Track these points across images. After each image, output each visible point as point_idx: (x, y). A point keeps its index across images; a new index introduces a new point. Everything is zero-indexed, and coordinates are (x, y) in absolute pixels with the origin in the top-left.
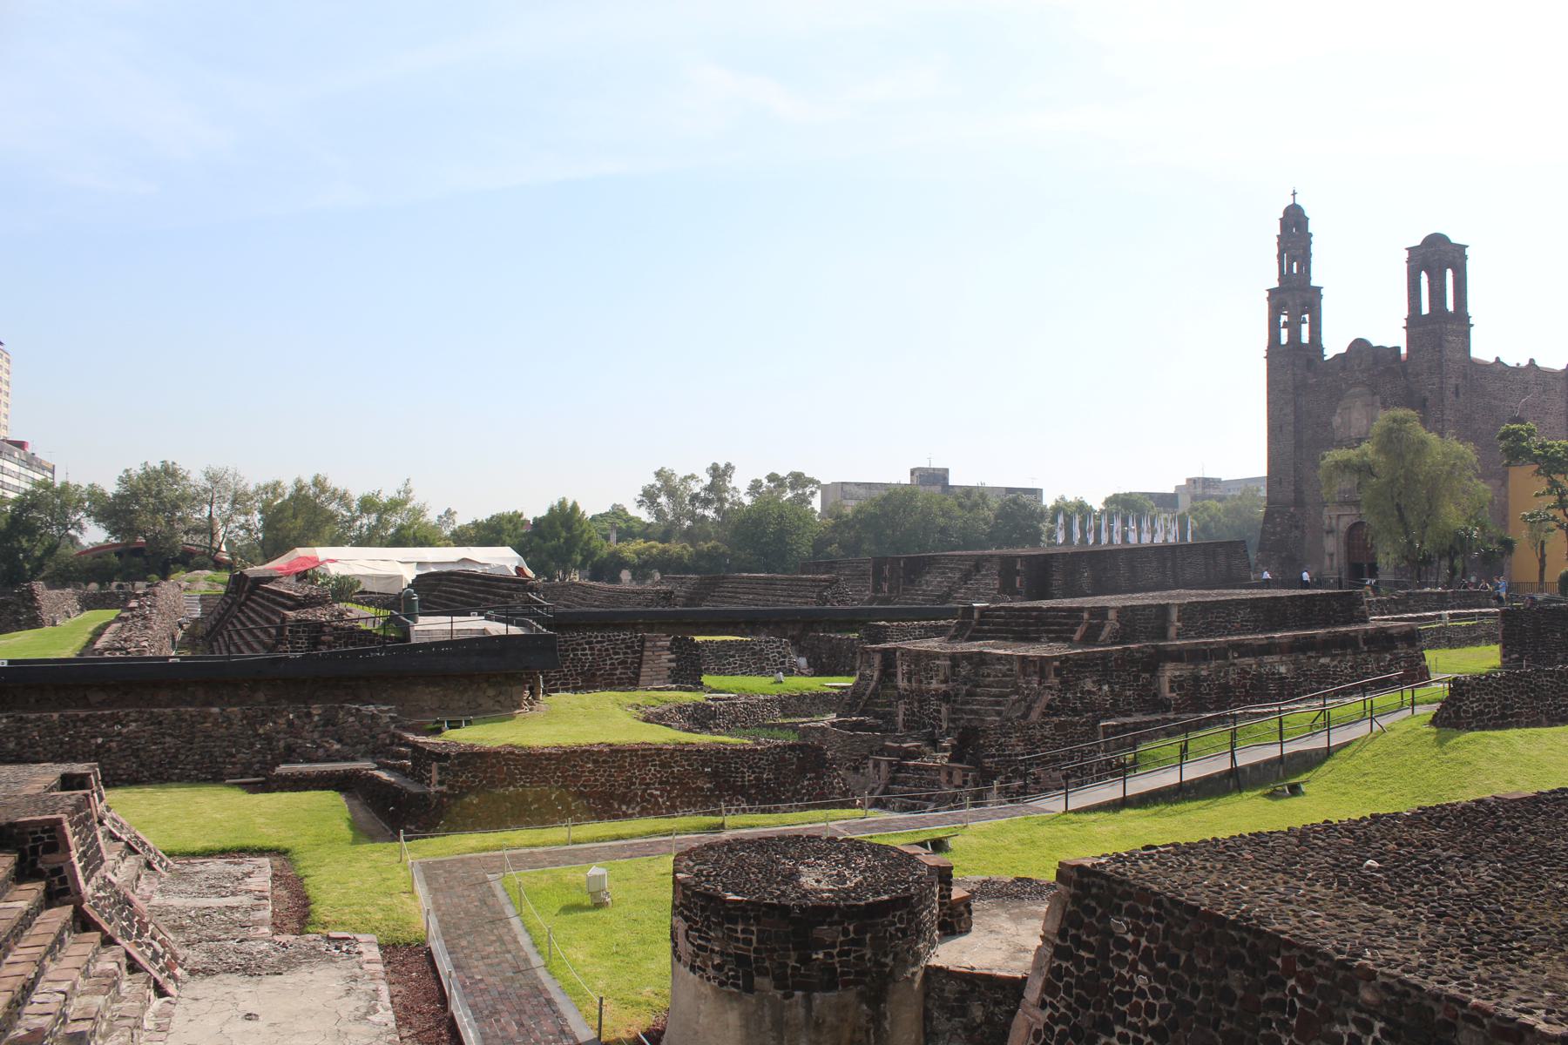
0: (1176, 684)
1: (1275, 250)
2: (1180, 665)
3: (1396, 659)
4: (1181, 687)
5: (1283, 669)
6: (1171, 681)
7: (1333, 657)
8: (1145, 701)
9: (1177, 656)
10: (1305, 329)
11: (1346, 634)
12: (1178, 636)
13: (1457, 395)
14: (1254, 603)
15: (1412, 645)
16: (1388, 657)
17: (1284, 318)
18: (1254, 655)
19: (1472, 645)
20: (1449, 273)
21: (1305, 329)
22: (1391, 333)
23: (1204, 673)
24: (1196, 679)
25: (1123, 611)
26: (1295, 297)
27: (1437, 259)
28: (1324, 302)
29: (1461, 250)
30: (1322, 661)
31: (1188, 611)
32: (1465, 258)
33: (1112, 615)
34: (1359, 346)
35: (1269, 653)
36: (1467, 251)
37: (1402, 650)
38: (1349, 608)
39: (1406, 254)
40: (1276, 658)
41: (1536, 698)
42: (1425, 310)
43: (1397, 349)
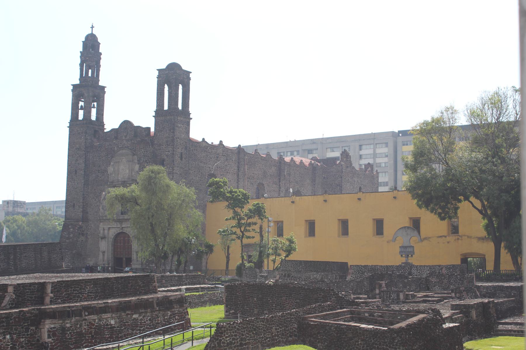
0: (52, 333)
1: (79, 61)
2: (55, 321)
3: (173, 315)
4: (54, 335)
5: (113, 322)
6: (49, 331)
7: (140, 314)
8: (32, 345)
9: (53, 315)
10: (94, 112)
11: (147, 300)
12: (52, 302)
13: (181, 159)
14: (95, 282)
15: (182, 306)
16: (169, 313)
17: (81, 104)
18: (97, 314)
19: (202, 306)
20: (180, 87)
21: (94, 112)
22: (145, 119)
23: (68, 325)
24: (63, 329)
25: (17, 287)
26: (88, 92)
27: (173, 78)
29: (187, 74)
30: (135, 316)
31: (58, 286)
32: (190, 79)
33: (10, 289)
34: (126, 125)
35: (105, 312)
36: (191, 76)
37: (177, 309)
38: (146, 284)
39: (157, 73)
40: (109, 315)
41: (256, 334)
42: (166, 107)
43: (149, 129)
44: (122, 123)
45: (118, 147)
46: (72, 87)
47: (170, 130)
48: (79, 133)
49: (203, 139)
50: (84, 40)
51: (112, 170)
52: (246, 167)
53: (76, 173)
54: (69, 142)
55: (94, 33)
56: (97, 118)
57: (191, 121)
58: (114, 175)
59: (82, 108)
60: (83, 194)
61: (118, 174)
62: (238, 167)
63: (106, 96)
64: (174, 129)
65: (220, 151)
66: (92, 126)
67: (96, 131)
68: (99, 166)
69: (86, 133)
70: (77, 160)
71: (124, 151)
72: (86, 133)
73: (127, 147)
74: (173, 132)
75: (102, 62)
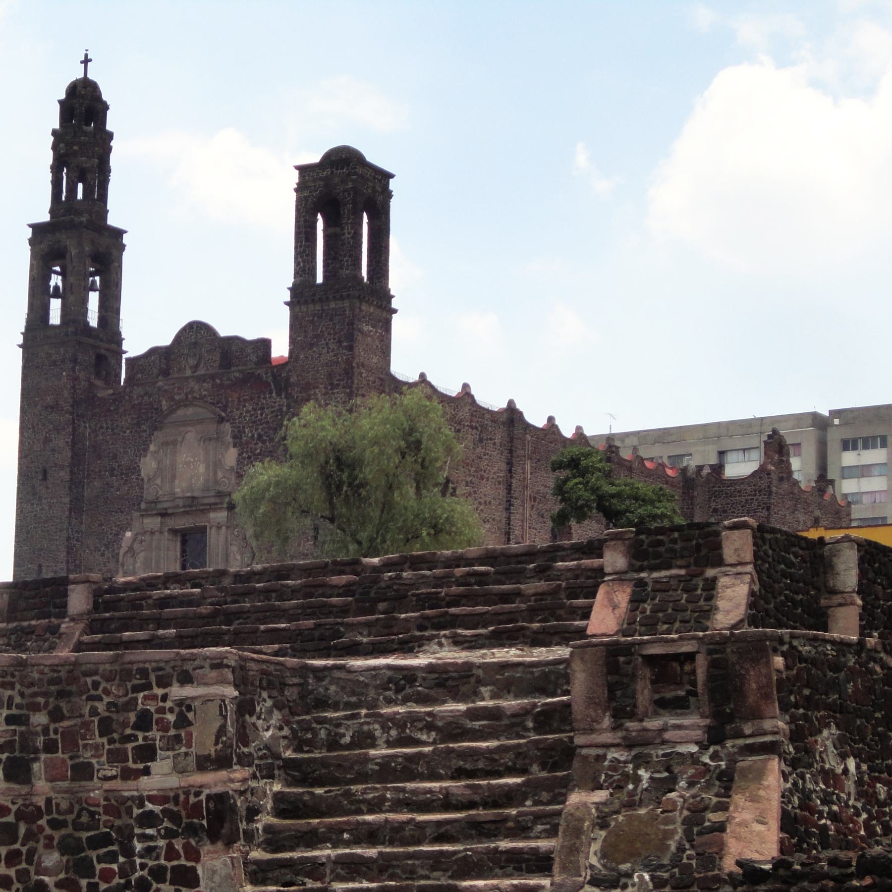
1: (48, 157)
17: (56, 280)
22: (259, 312)
26: (78, 242)
28: (127, 258)
32: (389, 195)
34: (196, 334)
36: (393, 184)
39: (294, 178)
43: (264, 345)
44: (184, 331)
45: (172, 399)
46: (29, 233)
47: (340, 342)
48: (54, 363)
49: (422, 376)
50: (63, 96)
51: (154, 465)
52: (528, 467)
53: (45, 478)
54: (23, 389)
55: (90, 76)
56: (102, 319)
57: (396, 320)
58: (158, 481)
59: (56, 294)
60: (68, 538)
61: (174, 477)
62: (510, 463)
63: (126, 257)
64: (351, 337)
65: (464, 413)
66: (91, 341)
67: (100, 359)
68: (115, 457)
69: (75, 361)
70: (47, 440)
71: (190, 411)
72: (75, 361)
73: (202, 398)
74: (351, 348)
75: (115, 160)
